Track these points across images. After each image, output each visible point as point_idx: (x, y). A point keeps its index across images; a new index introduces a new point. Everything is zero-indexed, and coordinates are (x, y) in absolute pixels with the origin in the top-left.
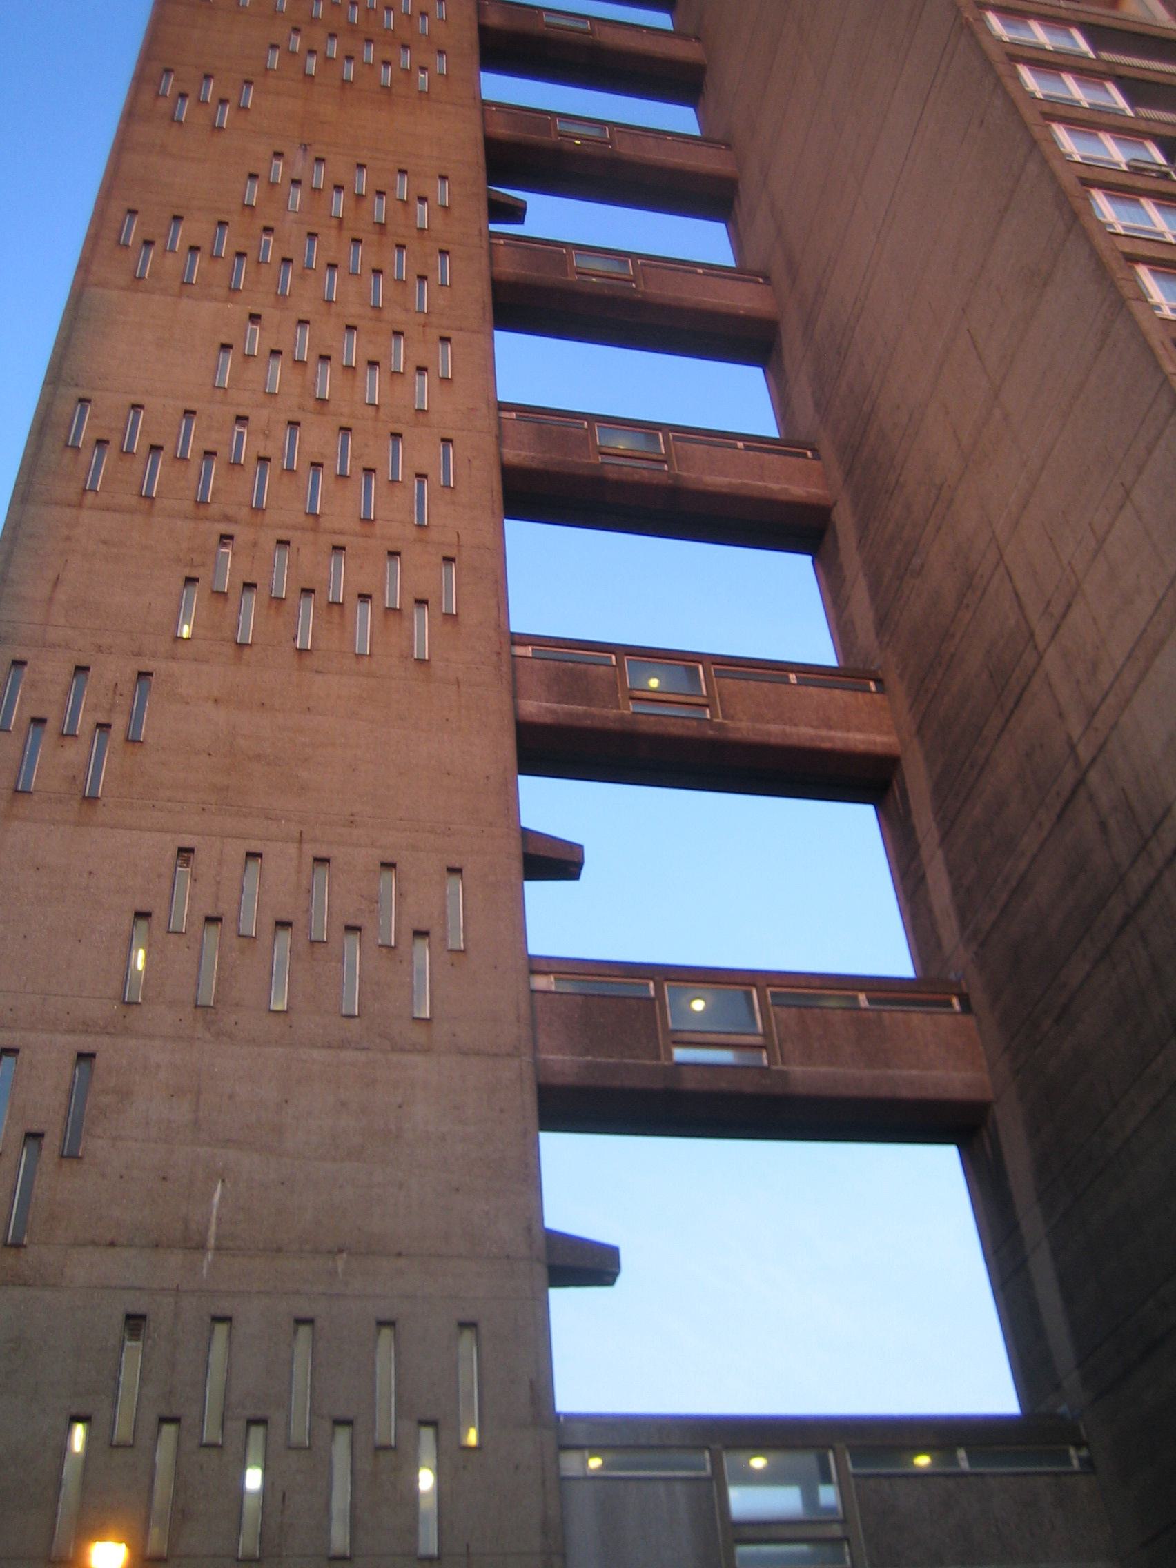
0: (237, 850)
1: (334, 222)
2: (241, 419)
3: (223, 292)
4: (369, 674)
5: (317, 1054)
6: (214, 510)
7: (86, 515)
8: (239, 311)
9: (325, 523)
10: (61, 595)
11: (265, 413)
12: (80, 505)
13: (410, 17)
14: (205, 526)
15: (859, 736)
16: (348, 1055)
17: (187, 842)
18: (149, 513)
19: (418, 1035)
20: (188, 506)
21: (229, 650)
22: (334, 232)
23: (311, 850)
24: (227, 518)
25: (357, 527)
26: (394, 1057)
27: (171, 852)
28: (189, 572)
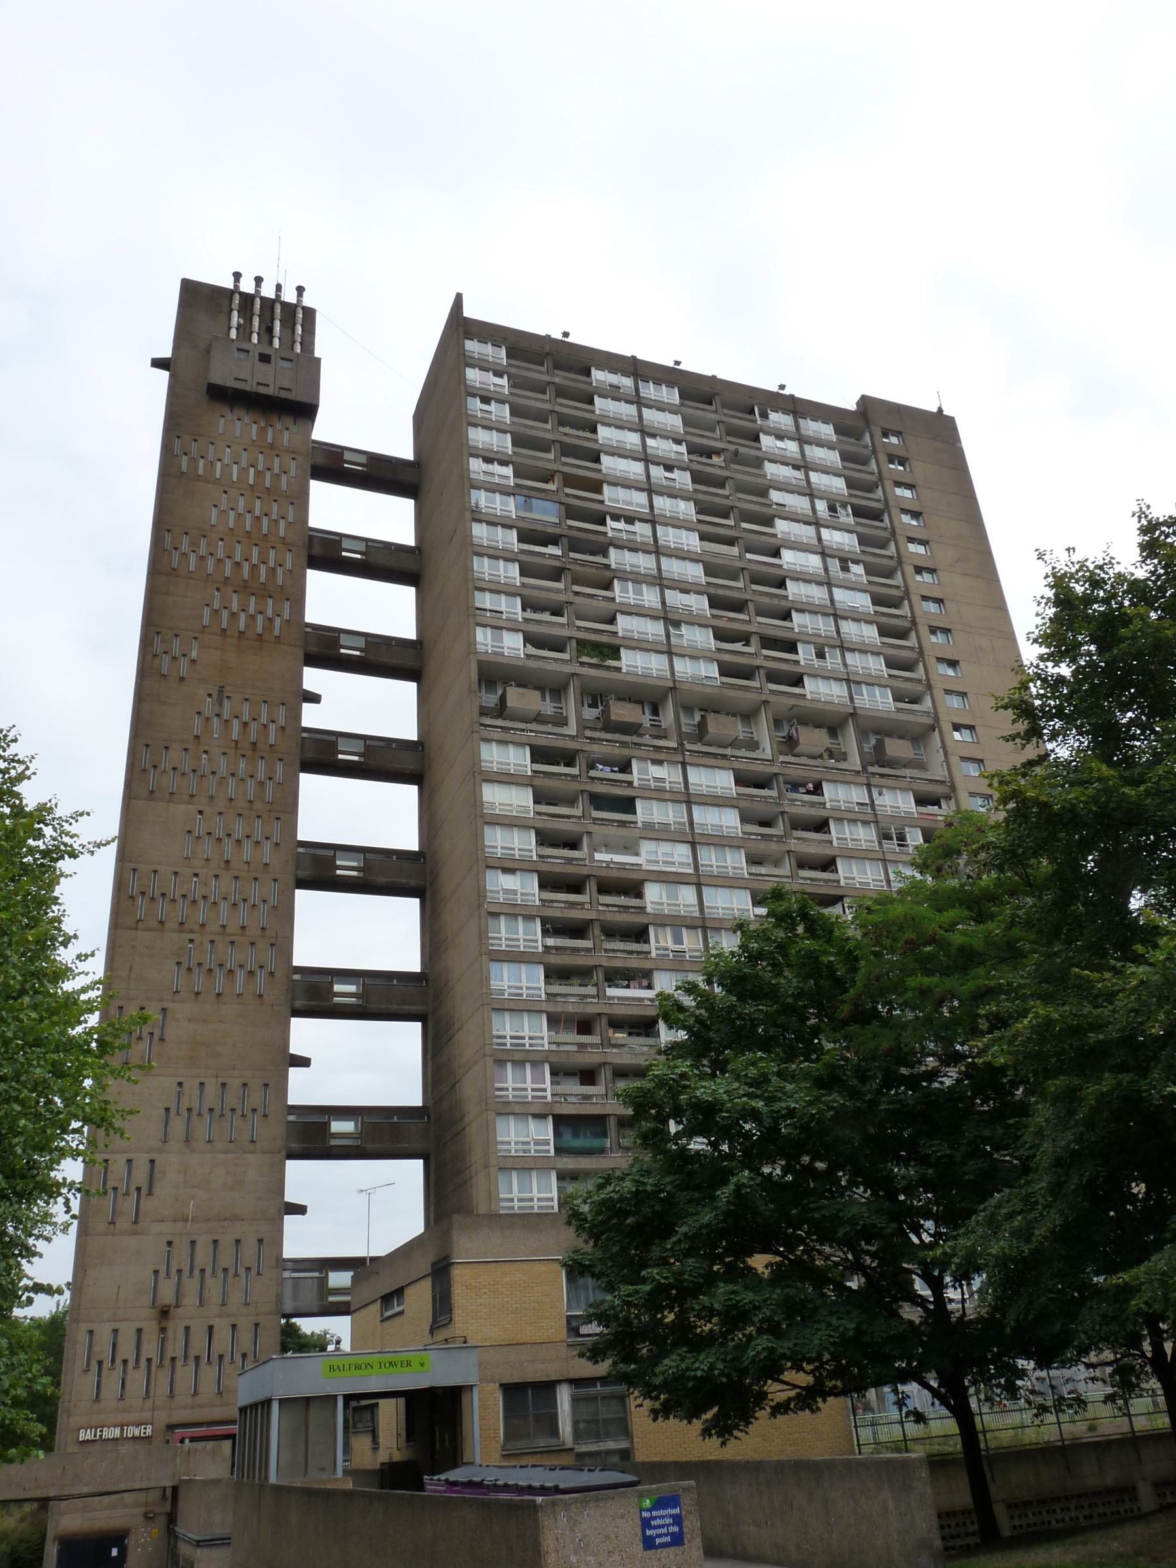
0: (197, 1082)
1: (234, 744)
2: (196, 875)
3: (186, 798)
4: (242, 1004)
5: (221, 1156)
6: (186, 927)
7: (139, 933)
8: (194, 808)
9: (228, 930)
10: (133, 976)
11: (205, 870)
12: (136, 929)
13: (276, 521)
14: (183, 935)
15: (414, 1008)
16: (230, 1155)
17: (180, 1080)
18: (162, 930)
19: (251, 1147)
20: (176, 926)
21: (193, 996)
22: (233, 751)
23: (221, 1080)
24: (192, 931)
25: (239, 932)
26: (244, 1155)
27: (175, 1085)
28: (178, 960)
